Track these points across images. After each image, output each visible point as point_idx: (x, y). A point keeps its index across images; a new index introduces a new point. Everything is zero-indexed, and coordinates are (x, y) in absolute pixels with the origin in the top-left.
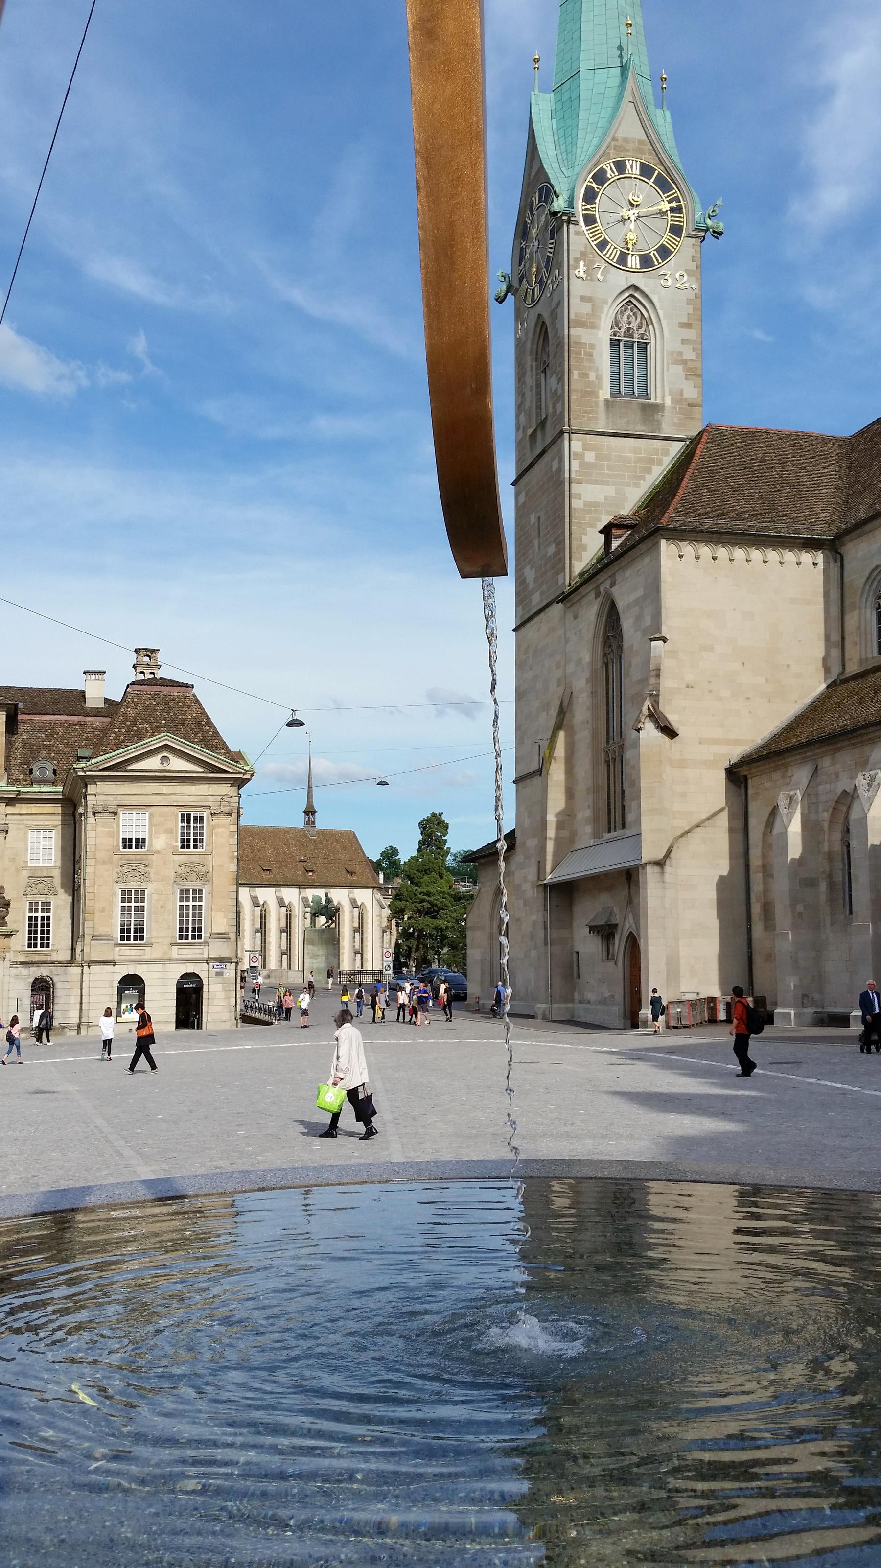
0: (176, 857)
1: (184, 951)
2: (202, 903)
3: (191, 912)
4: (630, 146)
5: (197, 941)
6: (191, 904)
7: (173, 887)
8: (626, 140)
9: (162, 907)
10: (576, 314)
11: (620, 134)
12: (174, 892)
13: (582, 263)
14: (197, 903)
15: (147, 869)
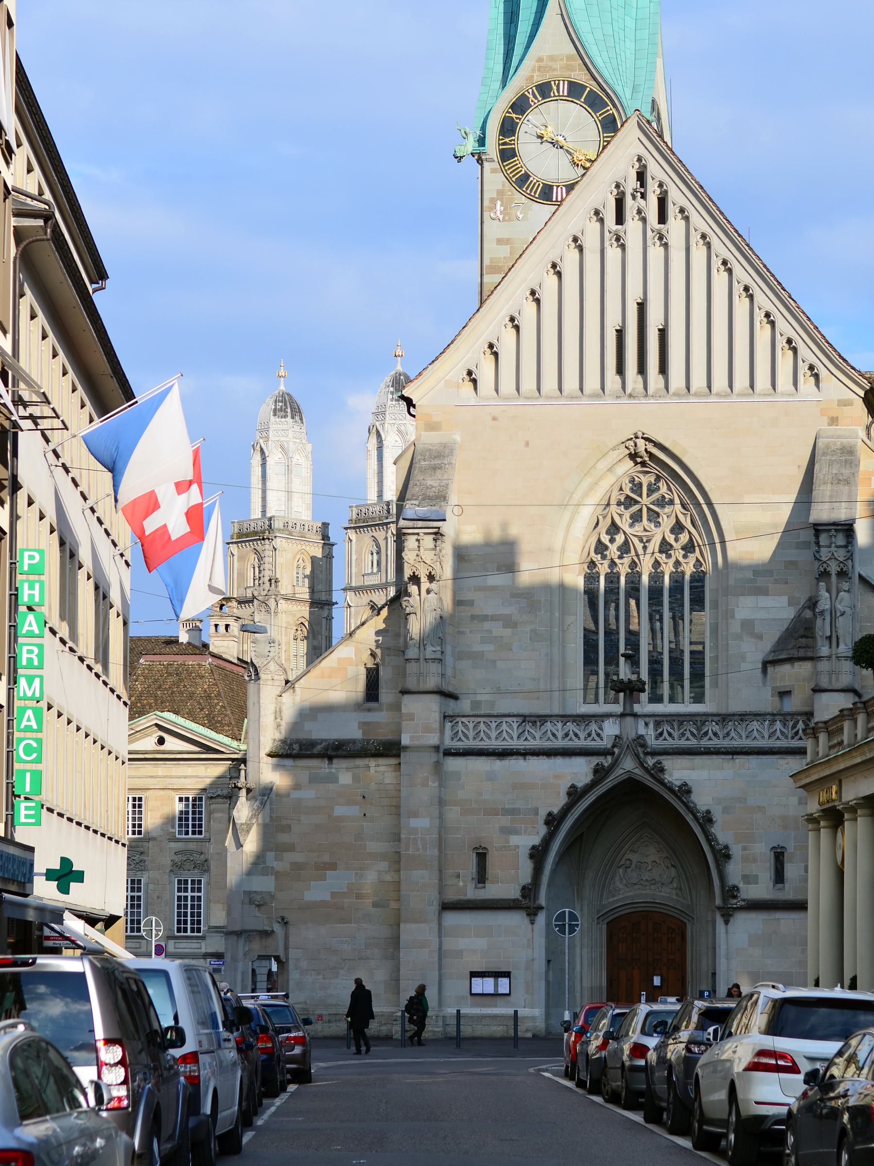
0: (173, 845)
1: (182, 945)
2: (177, 894)
3: (189, 903)
4: (557, 65)
5: (196, 934)
6: (189, 894)
7: (170, 876)
8: (552, 58)
9: (158, 897)
10: (491, 259)
11: (545, 54)
12: (171, 883)
13: (499, 203)
14: (196, 894)
15: (142, 857)
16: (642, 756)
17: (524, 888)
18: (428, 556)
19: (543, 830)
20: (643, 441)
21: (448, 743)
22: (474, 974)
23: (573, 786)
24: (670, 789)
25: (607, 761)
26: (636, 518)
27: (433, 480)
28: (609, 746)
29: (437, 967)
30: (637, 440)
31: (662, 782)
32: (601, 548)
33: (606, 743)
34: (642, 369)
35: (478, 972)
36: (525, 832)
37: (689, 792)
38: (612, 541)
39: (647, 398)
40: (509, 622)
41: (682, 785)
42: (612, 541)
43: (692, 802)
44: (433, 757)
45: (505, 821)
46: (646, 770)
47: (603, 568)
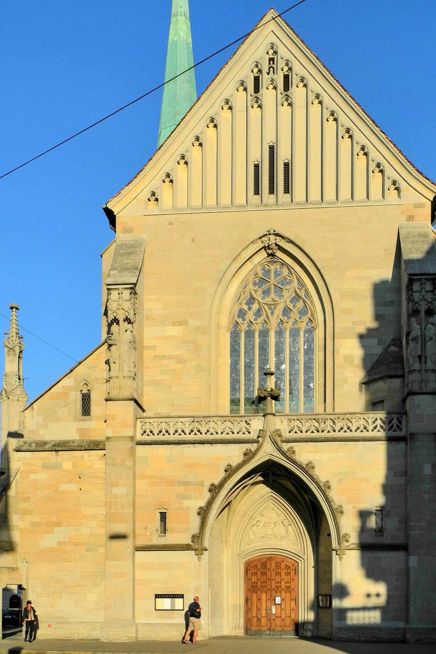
16: (279, 443)
17: (194, 536)
18: (127, 305)
19: (208, 496)
20: (273, 236)
21: (139, 437)
22: (157, 596)
23: (229, 465)
24: (300, 467)
25: (253, 447)
26: (266, 293)
27: (129, 260)
28: (255, 437)
29: (132, 591)
30: (270, 236)
31: (294, 462)
32: (242, 314)
33: (253, 436)
34: (272, 191)
35: (161, 595)
36: (195, 498)
37: (313, 468)
38: (250, 309)
39: (277, 207)
40: (180, 360)
41: (309, 463)
42: (250, 309)
43: (316, 476)
44: (130, 444)
45: (180, 489)
46: (283, 453)
47: (244, 327)
